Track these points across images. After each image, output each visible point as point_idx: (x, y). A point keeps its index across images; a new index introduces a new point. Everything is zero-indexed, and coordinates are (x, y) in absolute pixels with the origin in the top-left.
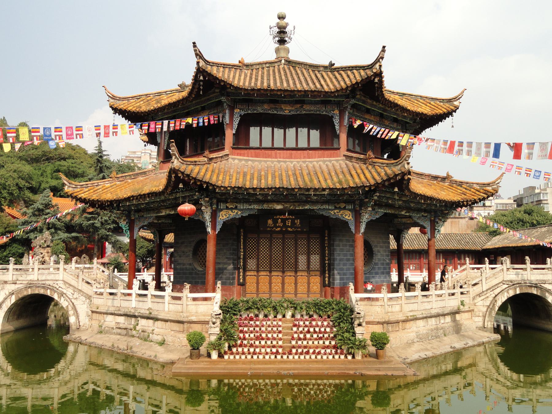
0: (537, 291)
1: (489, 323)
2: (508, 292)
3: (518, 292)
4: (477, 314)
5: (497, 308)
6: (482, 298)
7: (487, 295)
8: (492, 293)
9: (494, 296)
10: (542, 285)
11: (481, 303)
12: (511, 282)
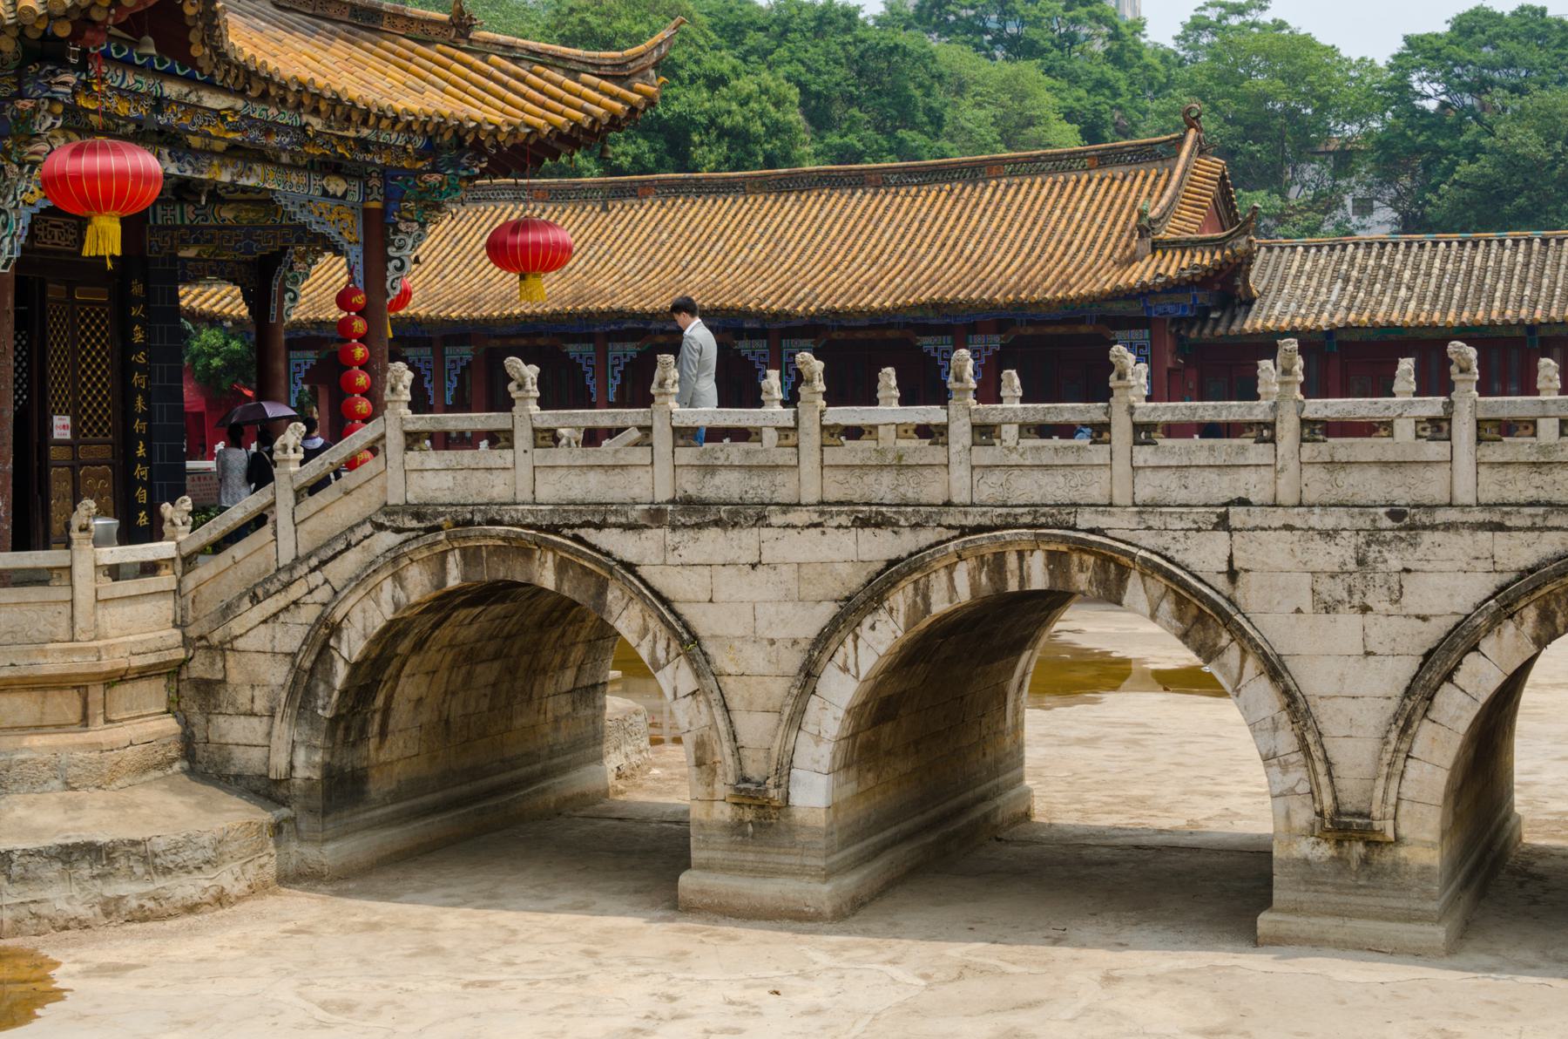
0: (562, 567)
1: (301, 756)
2: (397, 578)
3: (453, 580)
4: (243, 699)
5: (341, 673)
6: (270, 606)
7: (297, 591)
8: (317, 578)
9: (323, 594)
10: (590, 535)
11: (258, 639)
12: (418, 516)
